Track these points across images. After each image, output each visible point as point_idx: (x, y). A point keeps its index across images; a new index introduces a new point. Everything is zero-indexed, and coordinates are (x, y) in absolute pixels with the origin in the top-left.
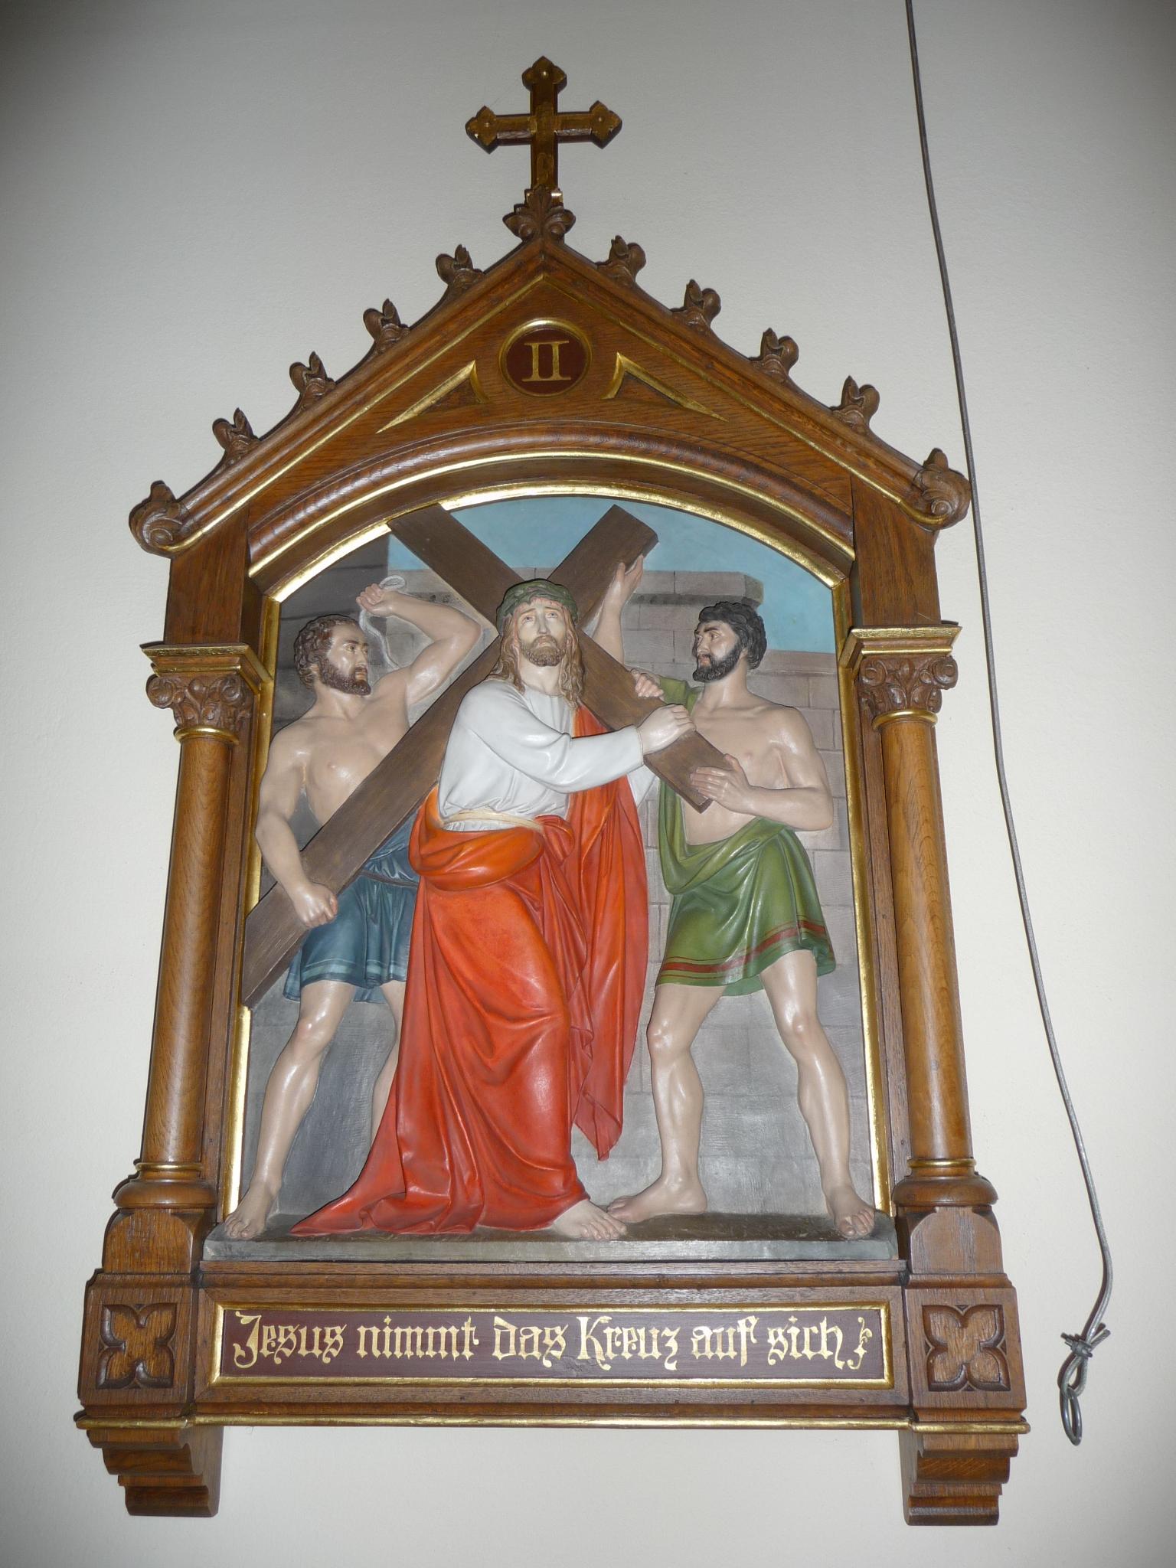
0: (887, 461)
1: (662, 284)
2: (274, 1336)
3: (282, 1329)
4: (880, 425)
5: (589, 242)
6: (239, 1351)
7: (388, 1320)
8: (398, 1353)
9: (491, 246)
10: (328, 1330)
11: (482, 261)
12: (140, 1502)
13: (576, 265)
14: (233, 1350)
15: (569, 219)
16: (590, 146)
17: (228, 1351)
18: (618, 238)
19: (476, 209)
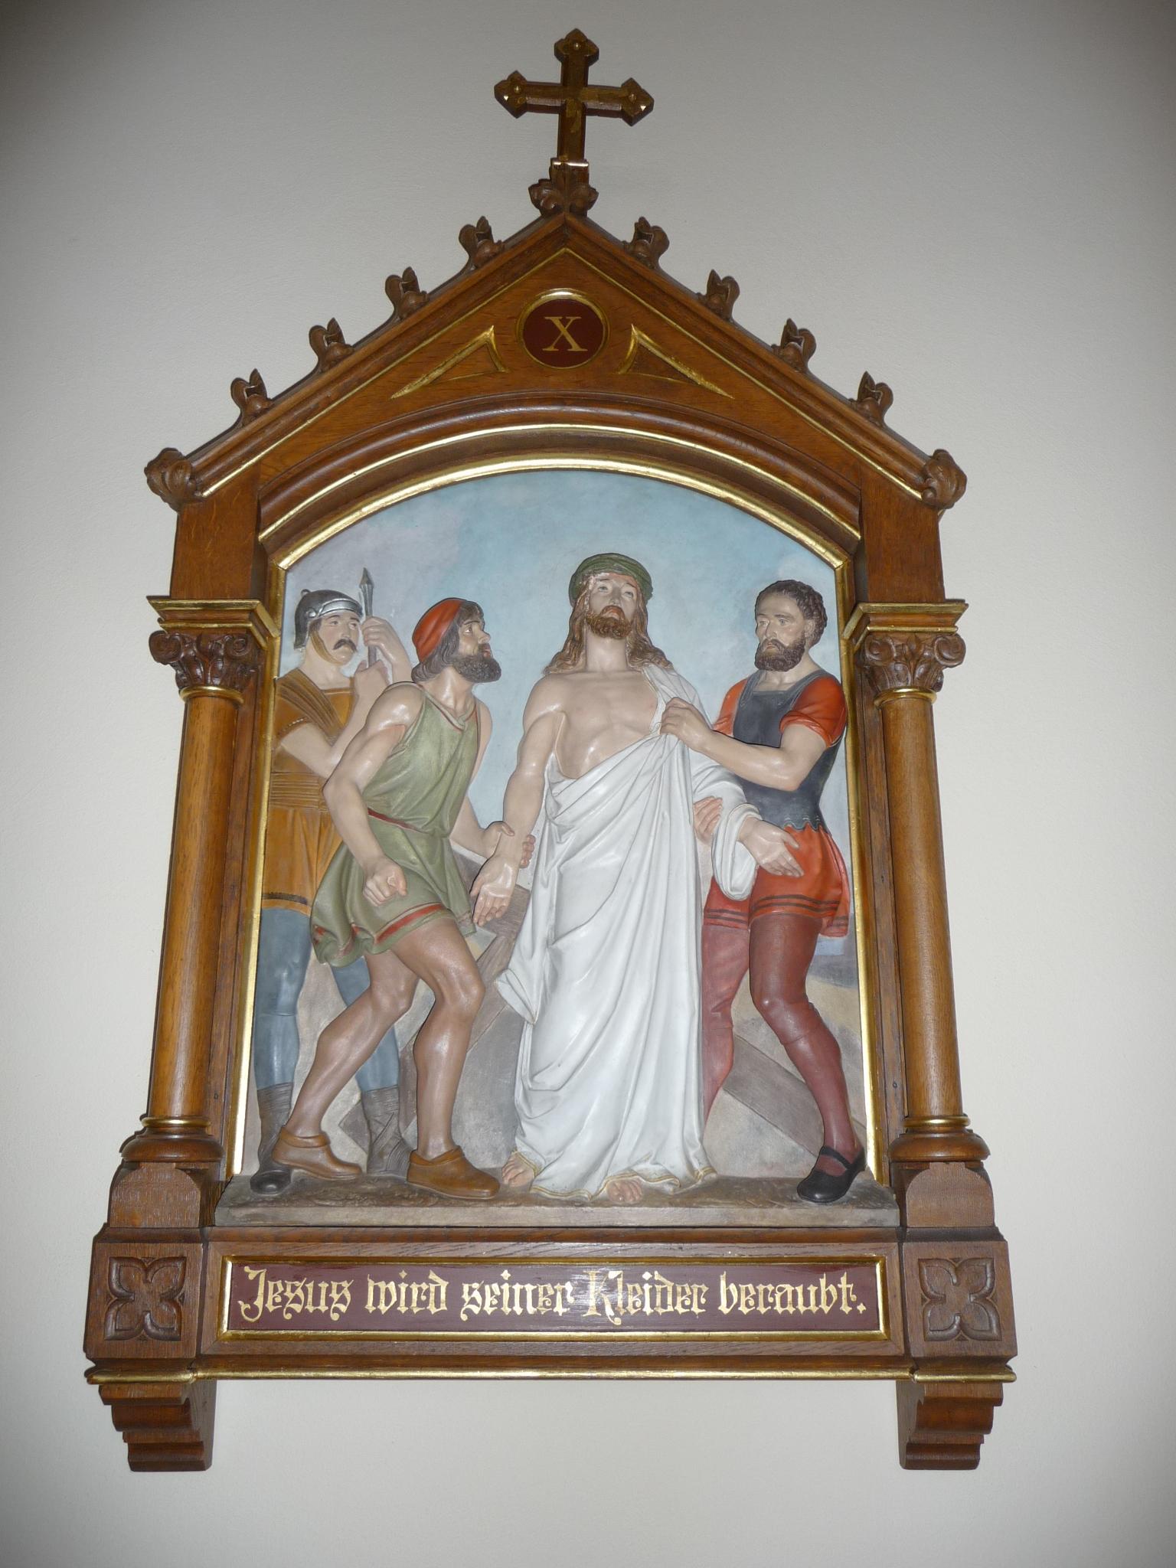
0: (899, 451)
1: (686, 268)
2: (281, 1289)
3: (289, 1284)
4: (892, 418)
5: (613, 218)
6: (244, 1306)
7: (403, 1274)
8: (802, 1308)
9: (513, 216)
10: (335, 1285)
11: (501, 233)
12: (142, 1459)
13: (598, 243)
14: (239, 1307)
15: (591, 197)
16: (619, 122)
17: (234, 1308)
18: (642, 220)
19: (499, 179)
